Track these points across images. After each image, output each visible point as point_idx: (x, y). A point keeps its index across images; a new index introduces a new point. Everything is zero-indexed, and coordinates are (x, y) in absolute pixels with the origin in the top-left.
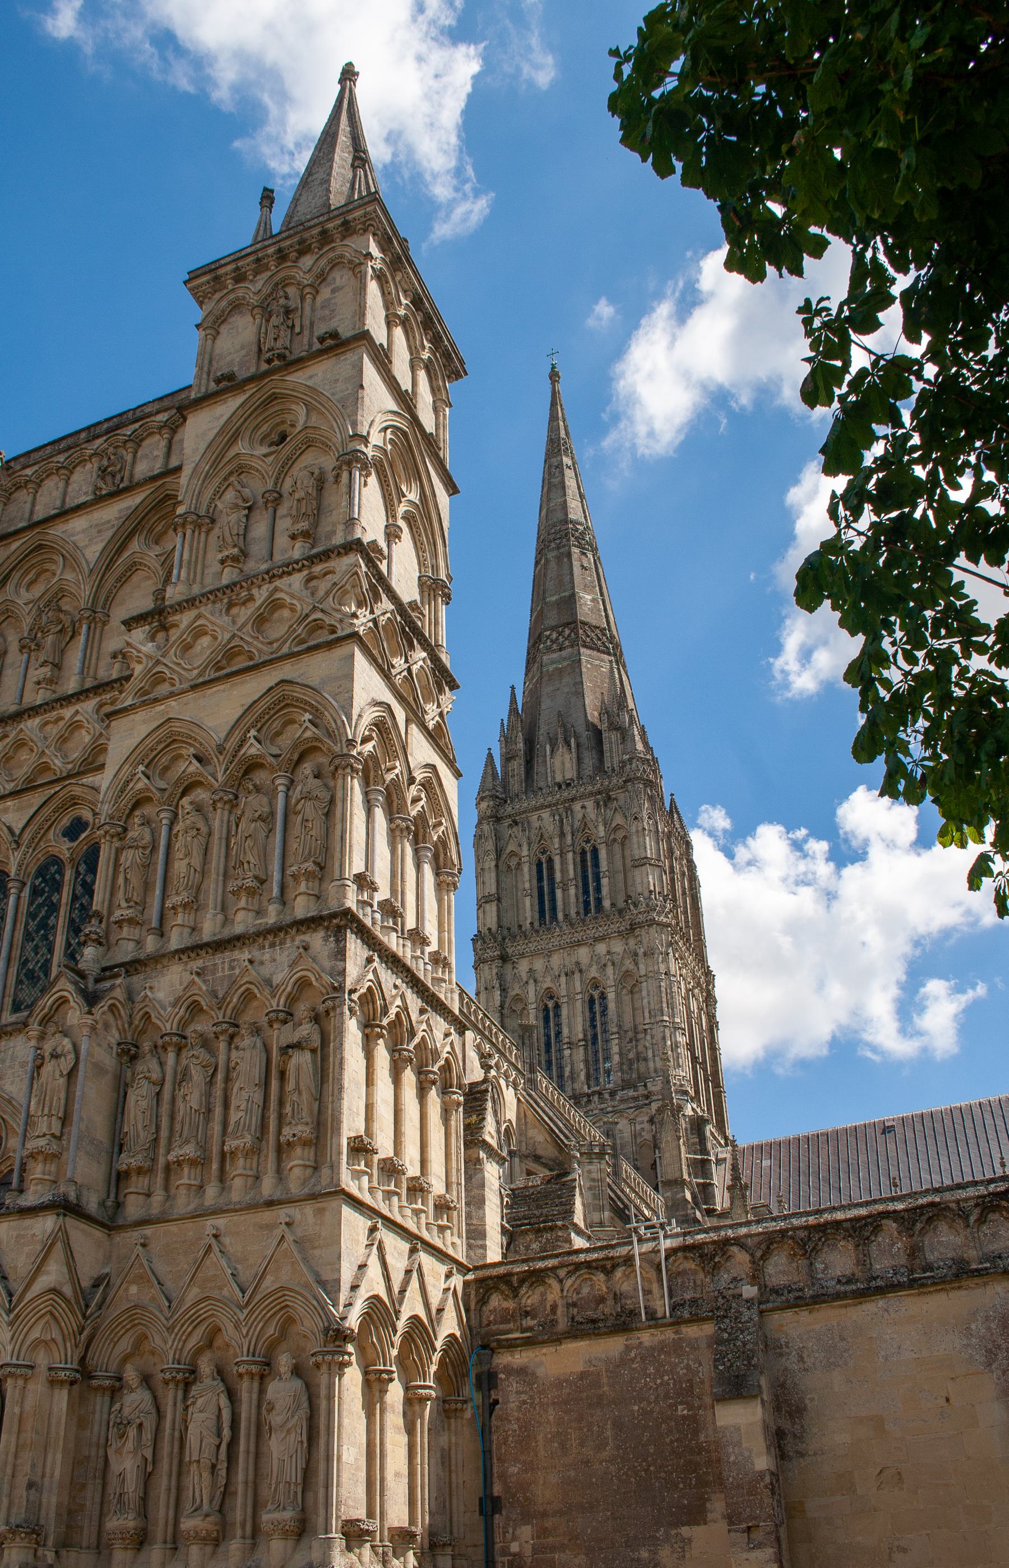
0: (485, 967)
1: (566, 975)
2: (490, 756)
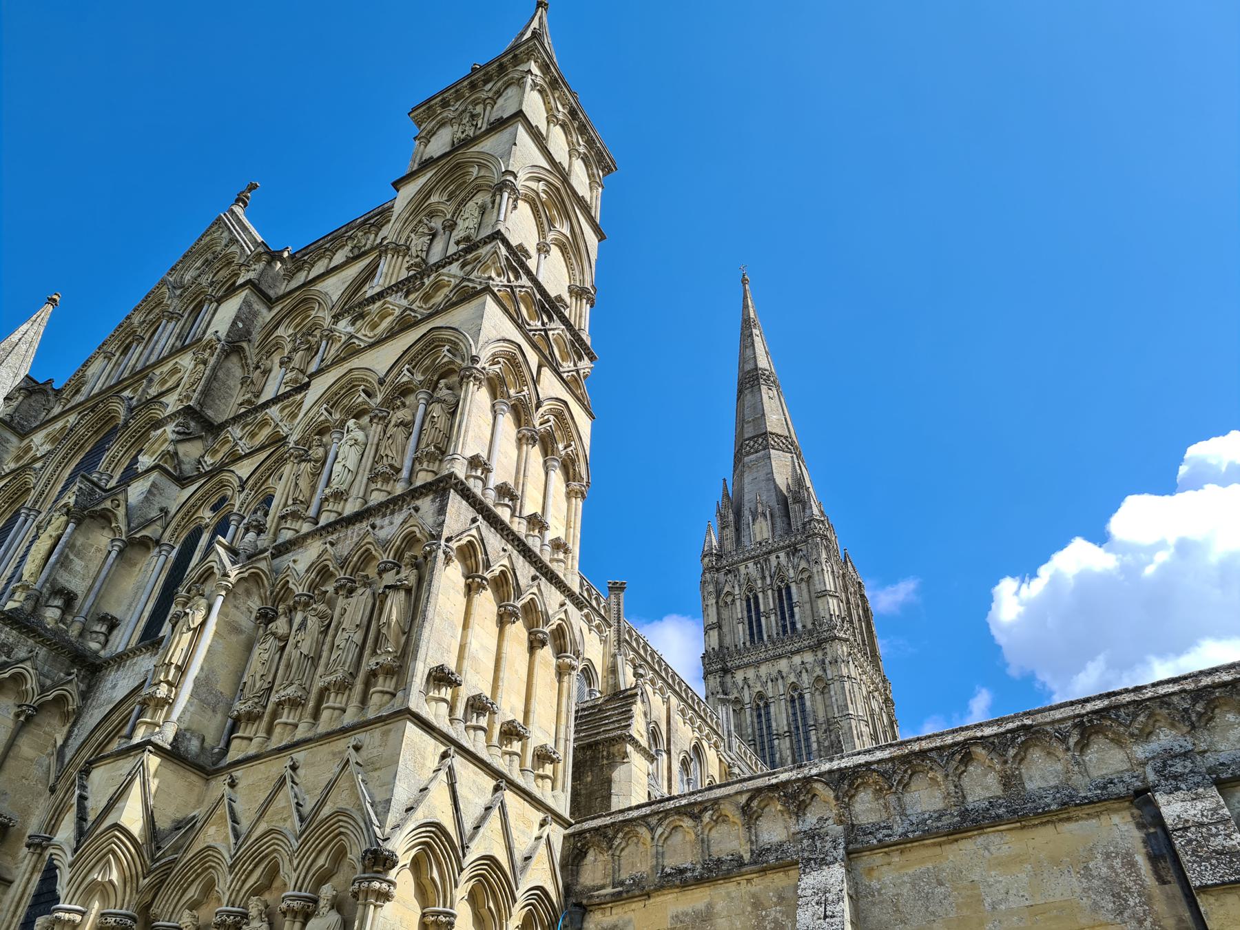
0: (711, 678)
1: (772, 681)
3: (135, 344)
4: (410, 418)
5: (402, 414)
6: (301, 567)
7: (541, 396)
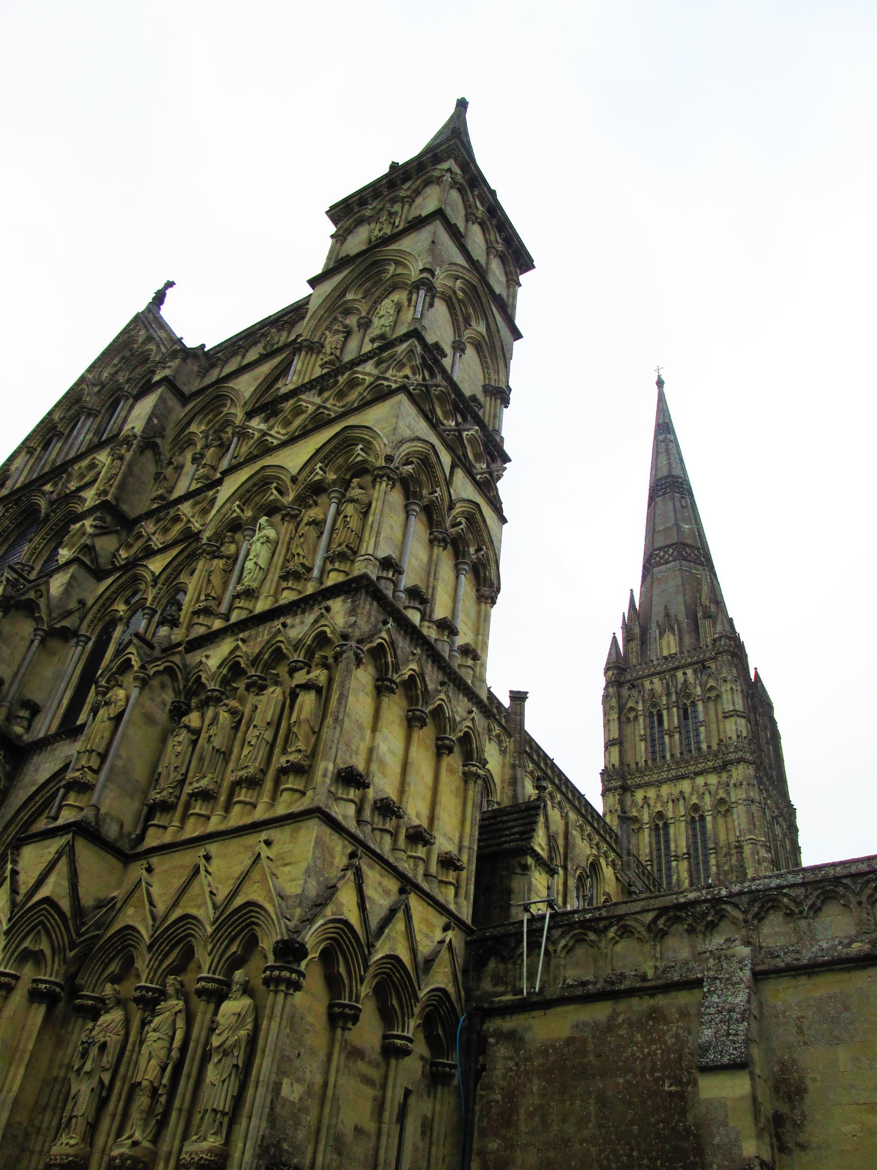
1: (673, 801)
2: (614, 639)
4: (321, 517)
5: (313, 513)
6: (213, 663)
7: (453, 498)
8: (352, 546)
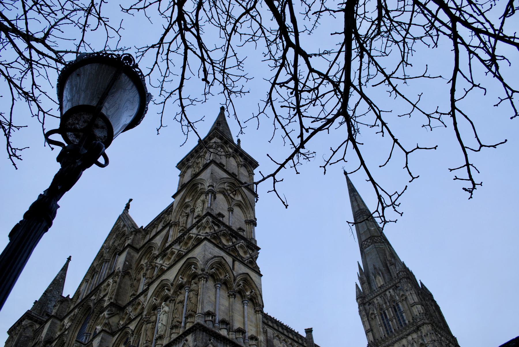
2: (357, 285)
3: (95, 275)
4: (183, 299)
5: (180, 298)
7: (235, 275)
8: (194, 310)
